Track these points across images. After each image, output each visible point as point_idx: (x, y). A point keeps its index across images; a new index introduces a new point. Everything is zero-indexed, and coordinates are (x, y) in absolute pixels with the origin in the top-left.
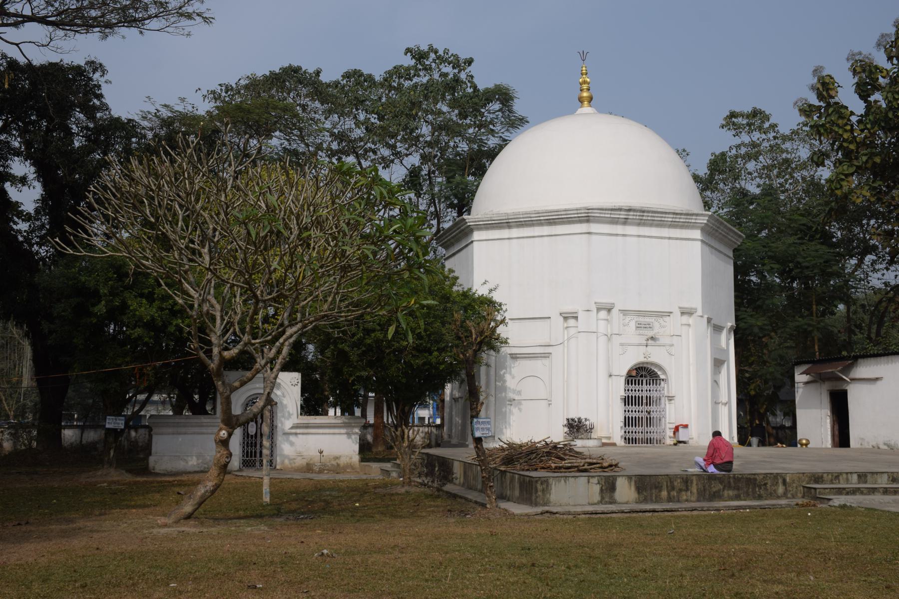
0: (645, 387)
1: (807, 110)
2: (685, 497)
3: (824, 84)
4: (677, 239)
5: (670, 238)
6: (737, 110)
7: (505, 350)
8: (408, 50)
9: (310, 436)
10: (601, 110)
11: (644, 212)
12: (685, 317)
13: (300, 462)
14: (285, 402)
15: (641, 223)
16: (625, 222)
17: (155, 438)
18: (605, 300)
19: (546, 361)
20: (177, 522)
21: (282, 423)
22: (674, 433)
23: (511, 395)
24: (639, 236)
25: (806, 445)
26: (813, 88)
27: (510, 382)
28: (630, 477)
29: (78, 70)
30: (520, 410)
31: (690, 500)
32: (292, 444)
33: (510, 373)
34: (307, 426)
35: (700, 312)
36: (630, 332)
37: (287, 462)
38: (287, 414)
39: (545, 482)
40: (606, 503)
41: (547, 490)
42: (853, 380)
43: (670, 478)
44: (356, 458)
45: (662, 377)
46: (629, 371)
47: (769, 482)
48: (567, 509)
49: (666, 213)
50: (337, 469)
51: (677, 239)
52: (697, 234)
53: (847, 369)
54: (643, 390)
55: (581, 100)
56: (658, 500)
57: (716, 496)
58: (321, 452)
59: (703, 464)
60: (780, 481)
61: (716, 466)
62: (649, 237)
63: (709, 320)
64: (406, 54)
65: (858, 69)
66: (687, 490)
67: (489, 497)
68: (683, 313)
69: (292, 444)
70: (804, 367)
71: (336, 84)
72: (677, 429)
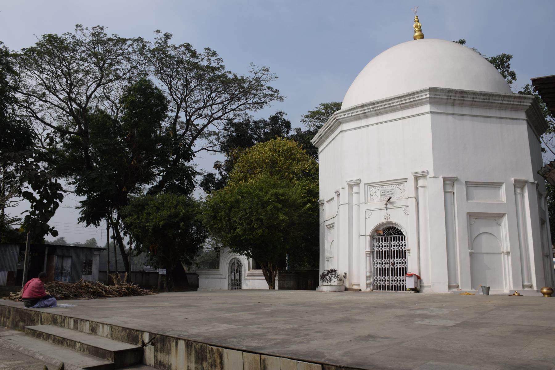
4: (409, 117)
5: (402, 118)
11: (374, 104)
15: (378, 113)
16: (366, 116)
24: (378, 123)
35: (432, 174)
36: (377, 201)
46: (376, 230)
51: (409, 117)
52: (427, 108)
54: (391, 245)
62: (385, 122)
63: (449, 182)
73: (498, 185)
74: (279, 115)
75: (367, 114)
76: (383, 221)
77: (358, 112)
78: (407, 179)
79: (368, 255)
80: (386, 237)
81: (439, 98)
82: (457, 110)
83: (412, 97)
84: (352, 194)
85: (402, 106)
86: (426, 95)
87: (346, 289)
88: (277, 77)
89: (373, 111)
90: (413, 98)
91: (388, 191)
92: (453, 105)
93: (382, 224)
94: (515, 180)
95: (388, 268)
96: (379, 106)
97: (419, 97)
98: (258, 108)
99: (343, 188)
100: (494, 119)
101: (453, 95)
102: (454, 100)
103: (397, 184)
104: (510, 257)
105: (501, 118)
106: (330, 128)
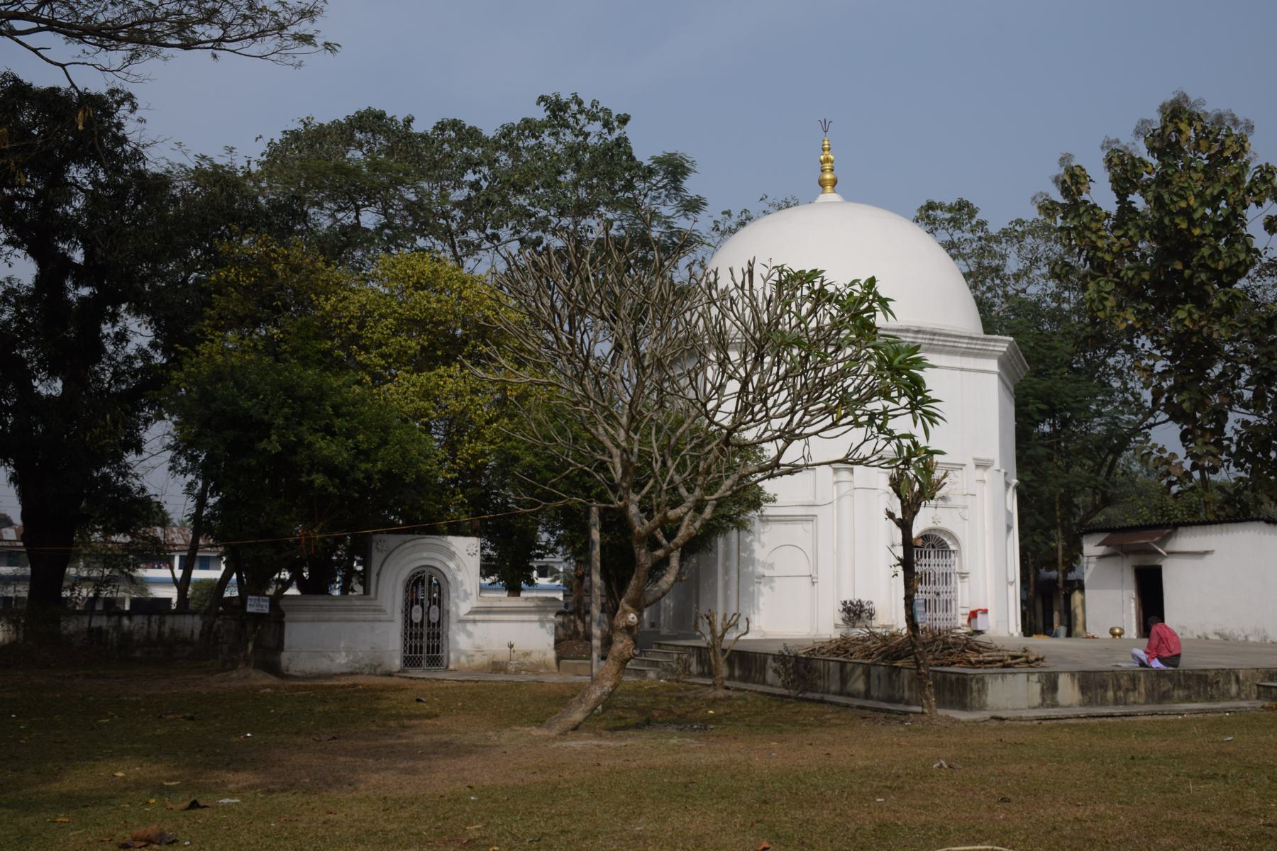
0: (933, 561)
1: (1049, 208)
2: (1132, 699)
3: (1073, 176)
4: (970, 370)
5: (962, 369)
6: (937, 201)
7: (768, 509)
8: (542, 99)
9: (492, 625)
10: (849, 197)
11: (935, 334)
12: (980, 471)
13: (479, 660)
14: (460, 577)
17: (289, 627)
19: (809, 526)
20: (564, 734)
21: (457, 606)
22: (969, 620)
23: (760, 570)
25: (1120, 635)
26: (1056, 180)
27: (760, 553)
28: (1072, 674)
29: (89, 100)
30: (772, 588)
31: (1138, 705)
32: (470, 635)
33: (759, 541)
34: (489, 611)
35: (997, 465)
37: (463, 659)
38: (462, 594)
39: (981, 680)
40: (1048, 706)
41: (982, 691)
42: (1171, 553)
43: (1116, 675)
44: (551, 655)
45: (952, 548)
47: (1221, 679)
48: (1017, 714)
49: (961, 337)
50: (535, 668)
51: (970, 370)
52: (993, 365)
53: (1164, 540)
55: (822, 184)
56: (1104, 702)
57: (1165, 697)
58: (511, 646)
59: (1144, 657)
60: (1233, 678)
61: (1162, 660)
64: (538, 103)
65: (1116, 160)
66: (1135, 689)
67: (927, 699)
68: (977, 466)
69: (470, 635)
70: (1101, 537)
71: (424, 137)
72: (973, 615)
76: (931, 525)
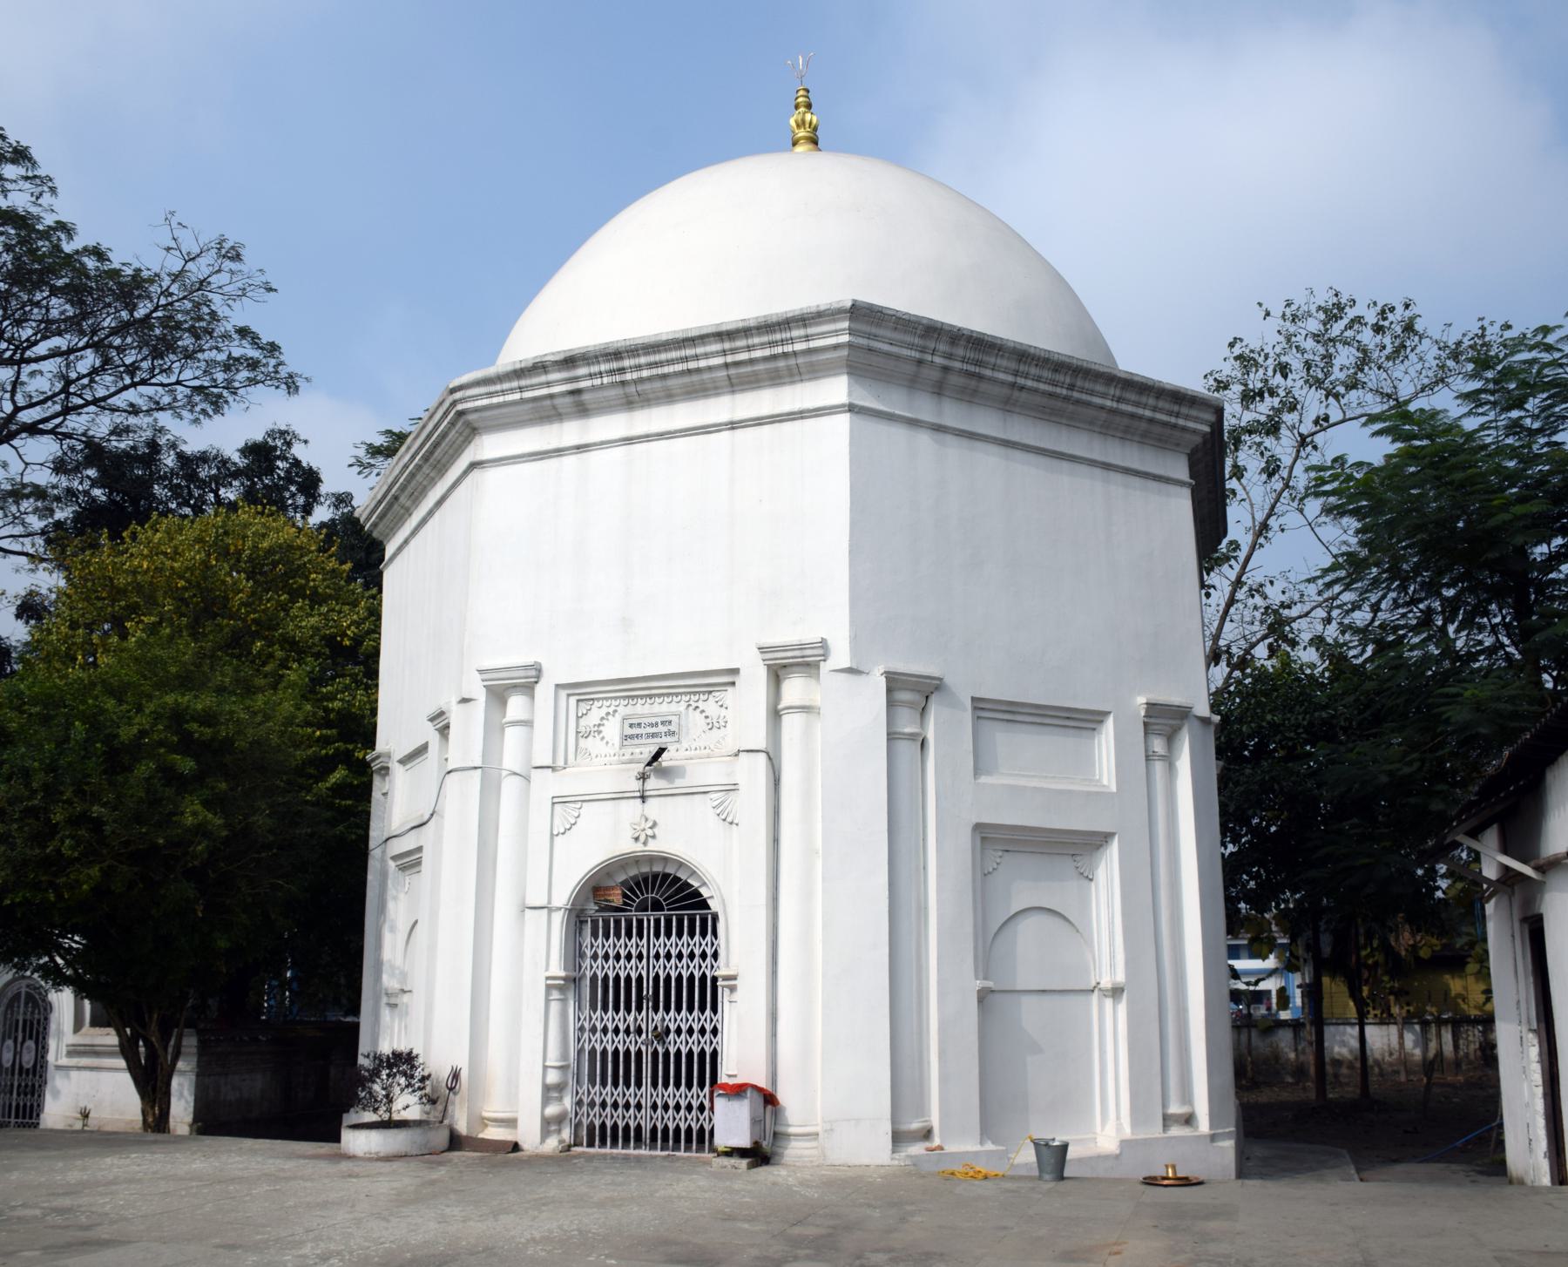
4: (759, 422)
5: (733, 426)
9: (104, 1075)
11: (616, 354)
15: (633, 399)
16: (580, 405)
18: (510, 656)
24: (629, 440)
35: (841, 656)
36: (606, 762)
51: (759, 422)
54: (658, 955)
62: (661, 436)
63: (911, 693)
73: (1085, 721)
74: (279, 443)
75: (586, 397)
77: (548, 384)
78: (735, 671)
79: (555, 995)
80: (634, 915)
81: (888, 354)
82: (953, 414)
83: (778, 336)
84: (503, 730)
85: (732, 371)
86: (836, 333)
87: (455, 1142)
88: (270, 290)
89: (613, 385)
90: (783, 342)
91: (652, 716)
92: (939, 390)
93: (623, 862)
94: (1151, 706)
95: (639, 1053)
96: (639, 367)
97: (807, 338)
98: (204, 411)
99: (465, 701)
100: (1084, 469)
101: (942, 347)
102: (946, 369)
103: (694, 691)
104: (1122, 1008)
105: (1107, 466)
106: (431, 452)
